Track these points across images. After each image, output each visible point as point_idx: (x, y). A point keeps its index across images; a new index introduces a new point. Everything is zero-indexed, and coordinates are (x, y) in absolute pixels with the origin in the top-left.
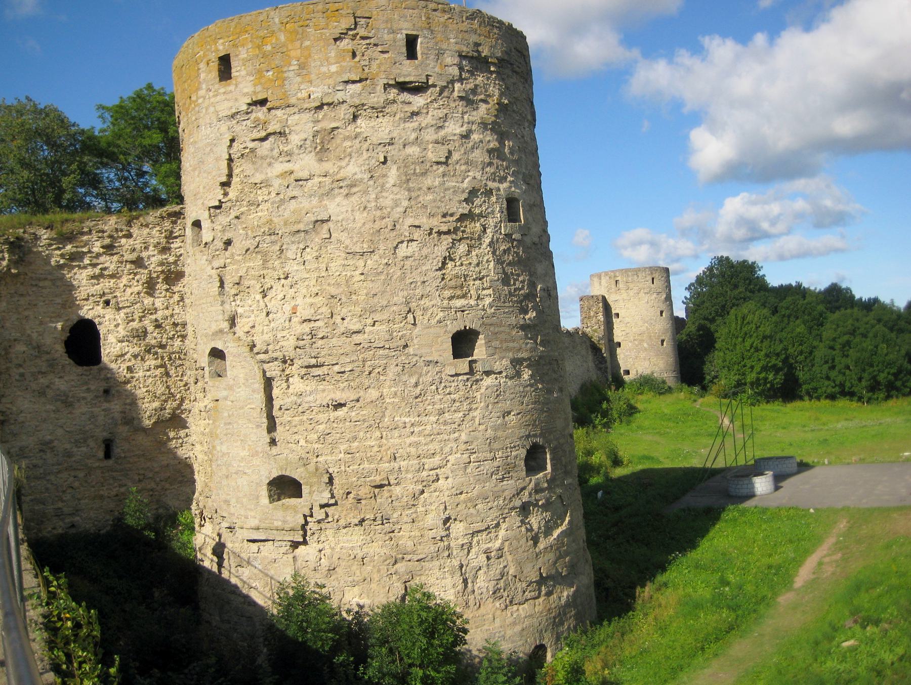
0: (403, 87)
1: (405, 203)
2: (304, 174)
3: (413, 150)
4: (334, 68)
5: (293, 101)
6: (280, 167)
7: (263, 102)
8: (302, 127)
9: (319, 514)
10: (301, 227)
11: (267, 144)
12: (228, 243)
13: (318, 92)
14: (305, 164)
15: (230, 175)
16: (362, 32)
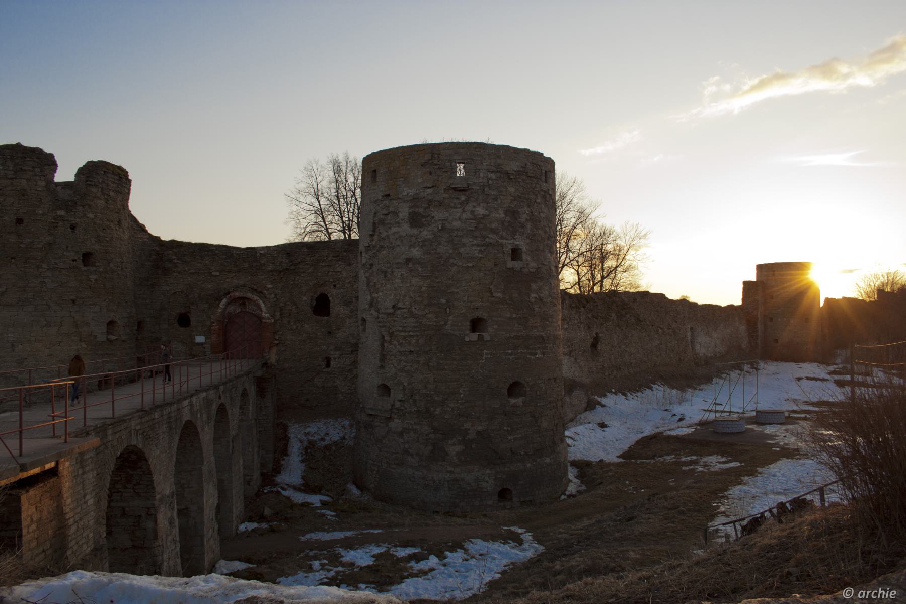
0: (455, 189)
1: (451, 251)
2: (403, 234)
3: (456, 224)
4: (420, 180)
5: (400, 196)
6: (394, 229)
7: (388, 195)
8: (404, 211)
9: (398, 404)
10: (400, 261)
11: (389, 217)
12: (372, 265)
13: (412, 192)
14: (406, 229)
15: (374, 231)
16: (436, 161)
